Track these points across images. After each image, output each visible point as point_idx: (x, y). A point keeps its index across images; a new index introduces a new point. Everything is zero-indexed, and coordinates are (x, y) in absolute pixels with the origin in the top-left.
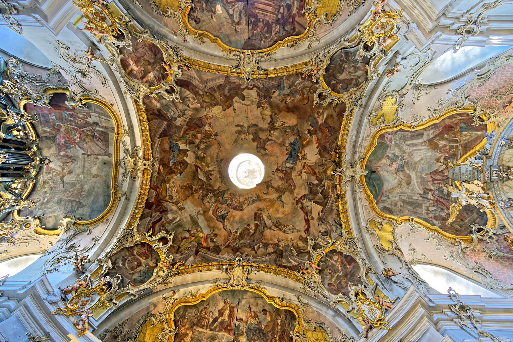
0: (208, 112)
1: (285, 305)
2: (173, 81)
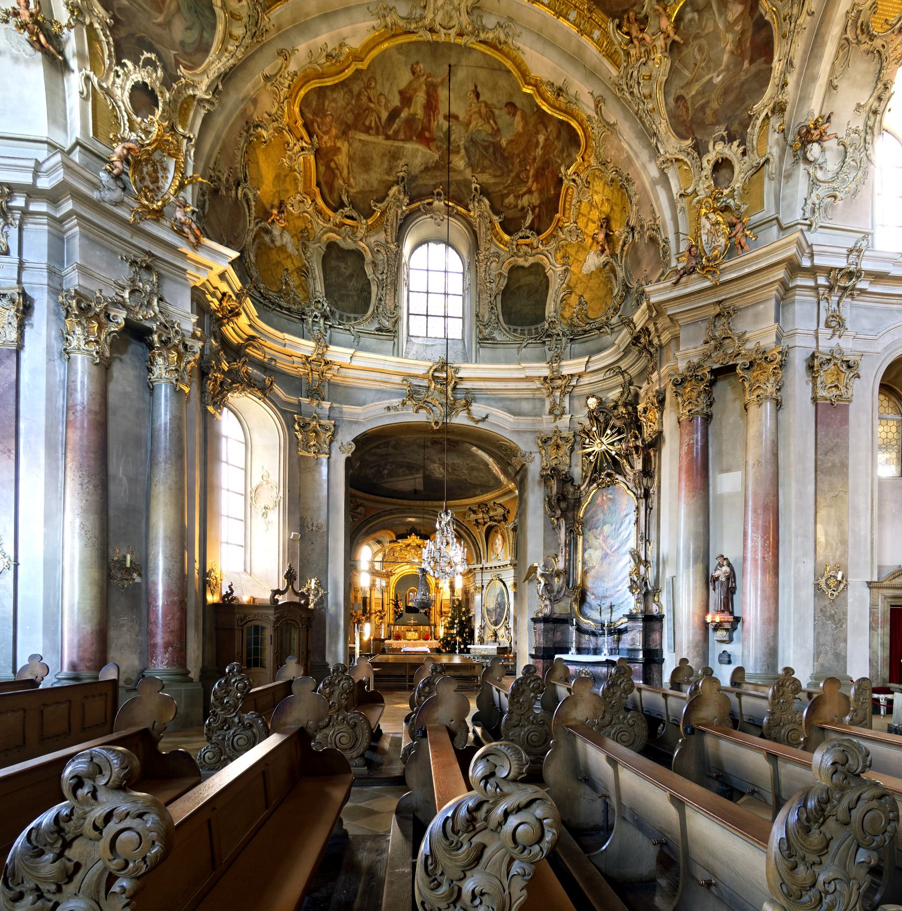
1: (563, 107)
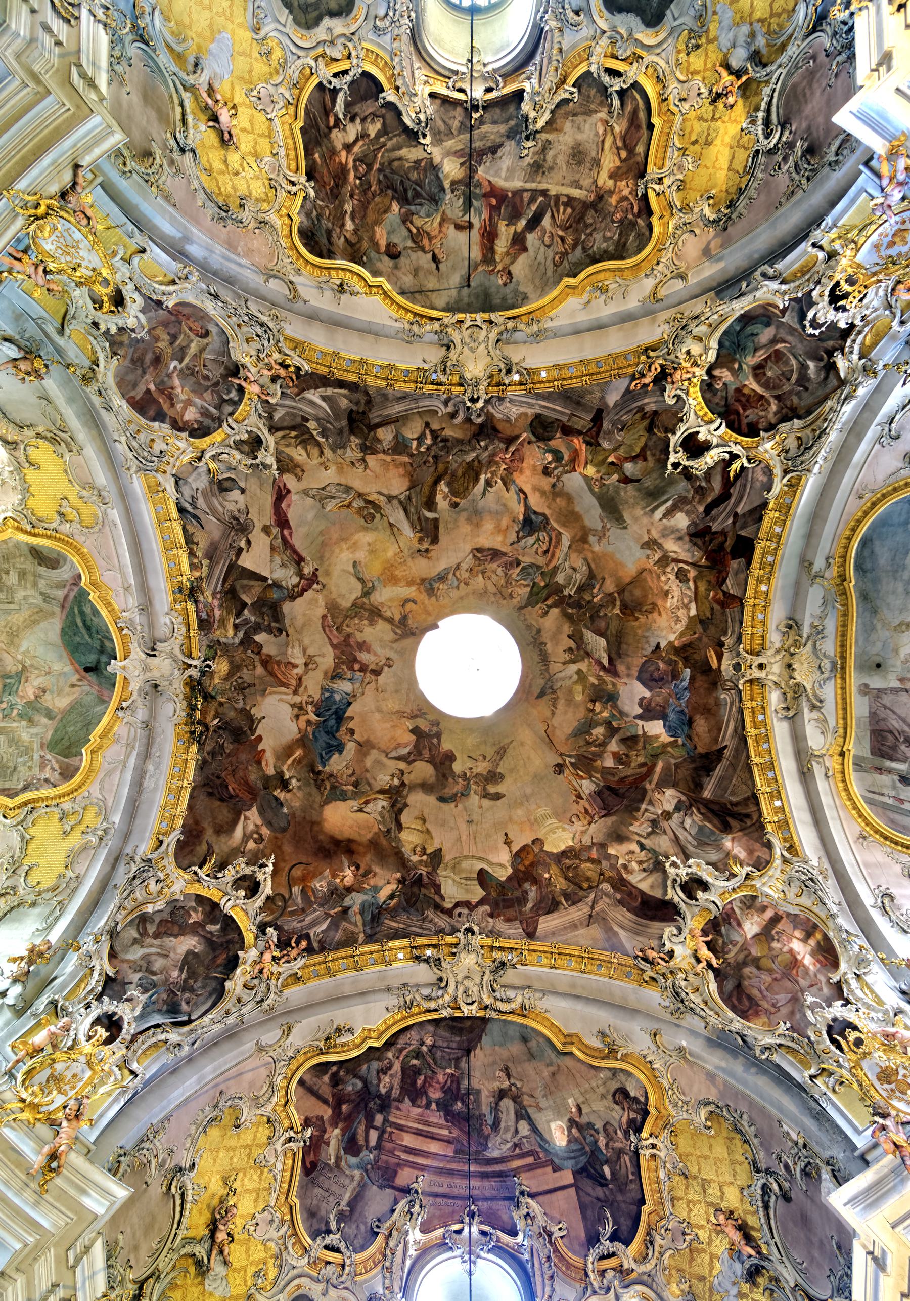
0: (584, 832)
2: (688, 916)
